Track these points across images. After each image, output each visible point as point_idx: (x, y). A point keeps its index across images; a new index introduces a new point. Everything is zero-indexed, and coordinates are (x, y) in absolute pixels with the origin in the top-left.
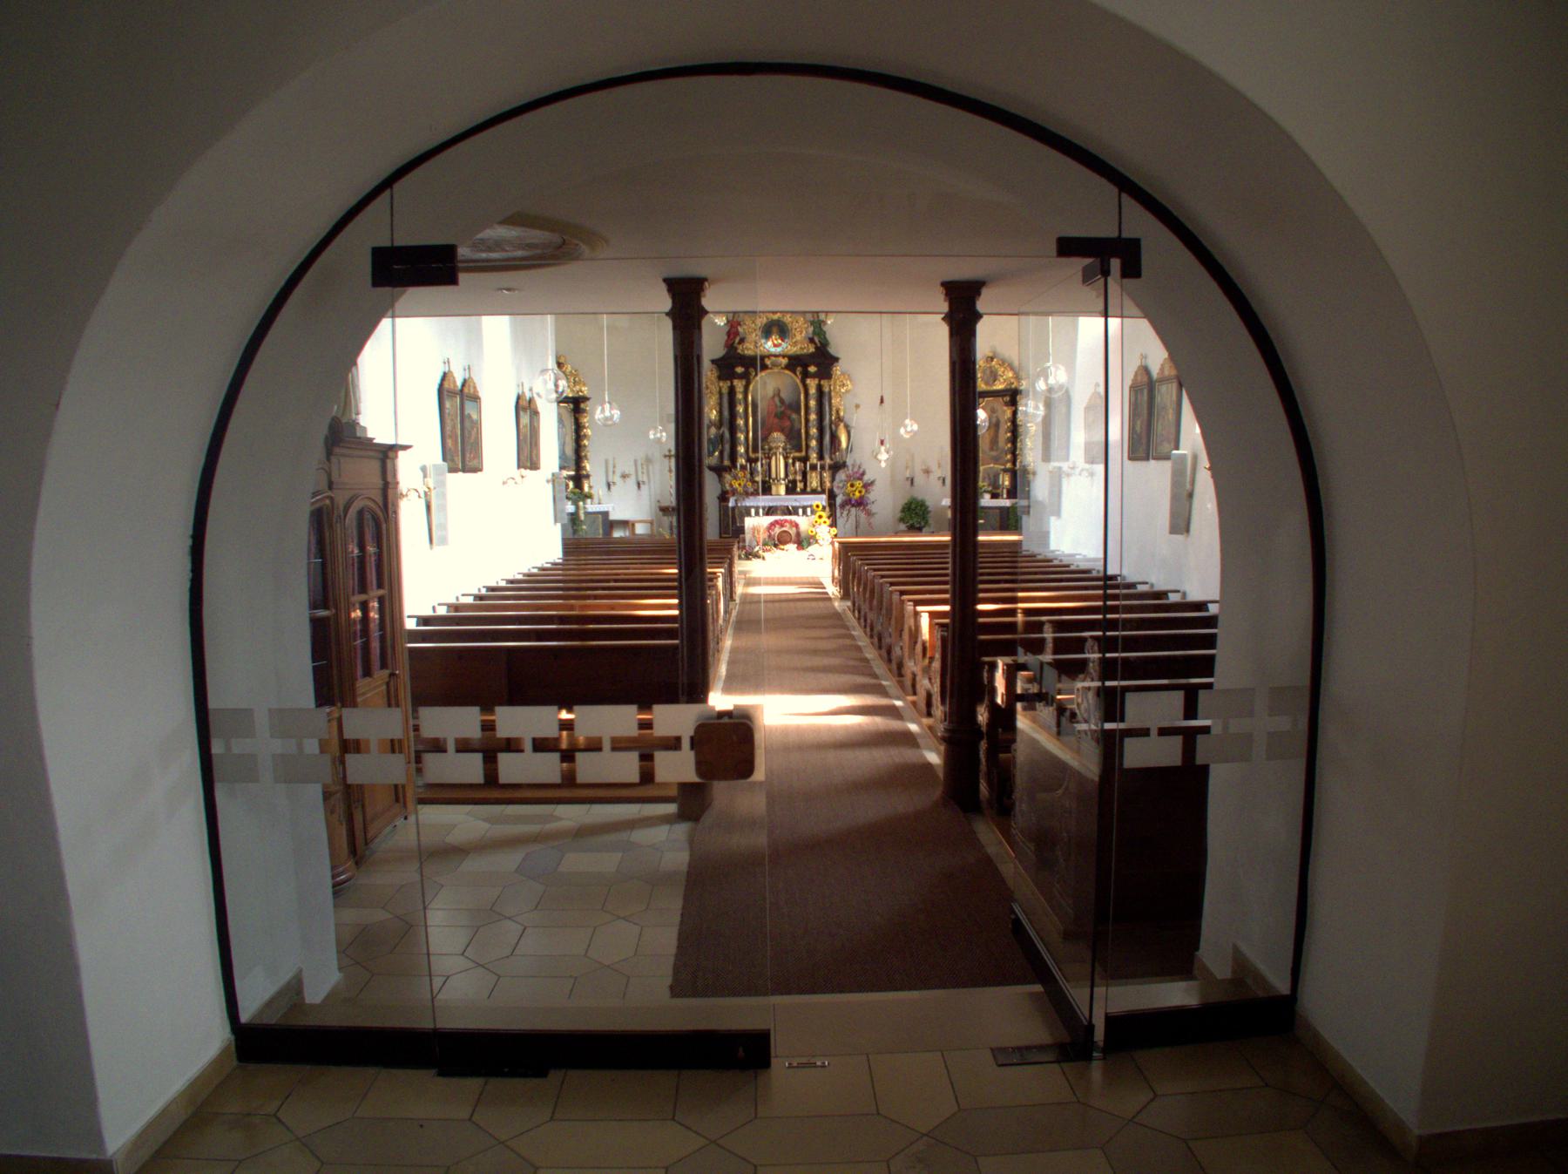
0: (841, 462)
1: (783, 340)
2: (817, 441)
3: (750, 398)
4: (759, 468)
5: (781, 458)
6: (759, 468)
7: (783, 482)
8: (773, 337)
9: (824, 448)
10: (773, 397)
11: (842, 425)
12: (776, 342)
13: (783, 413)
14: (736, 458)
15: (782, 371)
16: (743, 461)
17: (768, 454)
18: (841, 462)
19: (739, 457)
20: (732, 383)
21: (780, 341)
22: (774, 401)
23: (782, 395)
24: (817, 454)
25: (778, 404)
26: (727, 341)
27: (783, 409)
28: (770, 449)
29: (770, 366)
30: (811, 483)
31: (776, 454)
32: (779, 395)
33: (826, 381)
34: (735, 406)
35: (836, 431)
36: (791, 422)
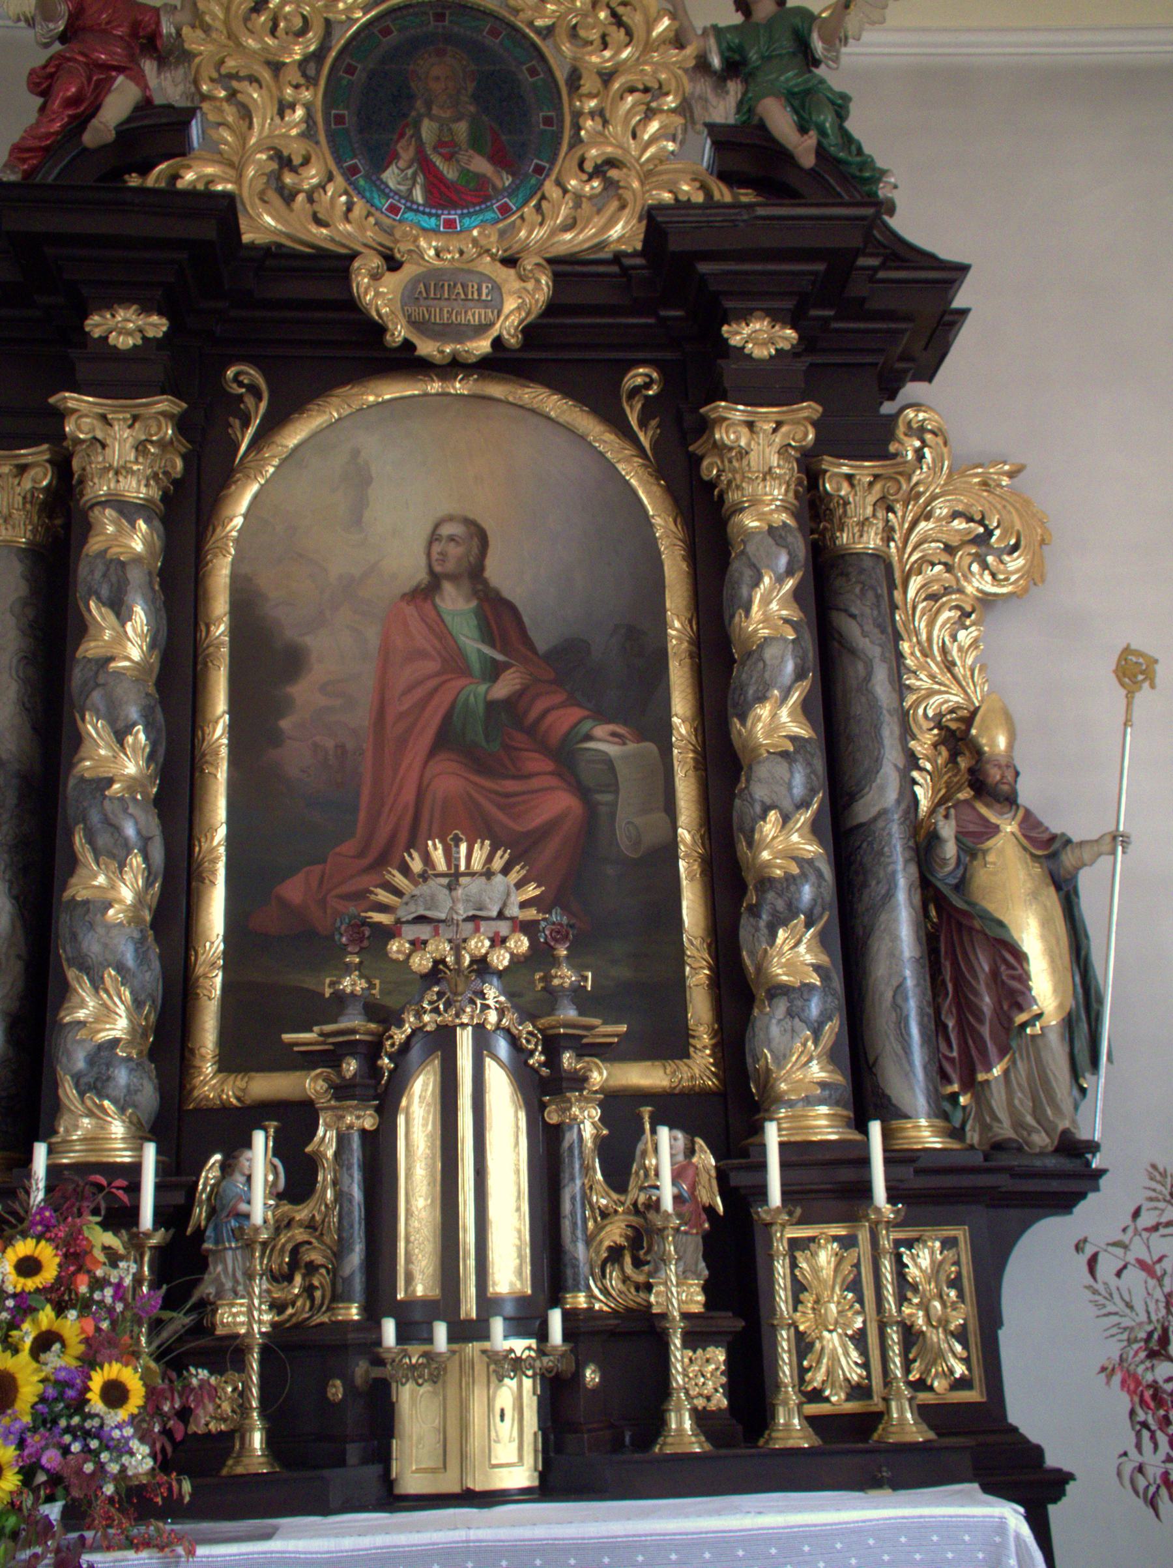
0: (1041, 1140)
1: (500, 159)
2: (823, 940)
3: (221, 572)
4: (259, 1208)
5: (499, 1083)
6: (259, 1208)
7: (521, 1346)
8: (428, 130)
9: (882, 1021)
10: (429, 590)
11: (1009, 827)
12: (449, 172)
13: (511, 707)
14: (56, 1107)
15: (496, 390)
16: (118, 1128)
17: (371, 1051)
18: (1041, 1140)
19: (68, 1092)
20: (62, 466)
21: (481, 165)
22: (440, 630)
23: (496, 572)
24: (832, 1057)
25: (472, 644)
26: (32, 127)
27: (502, 689)
28: (387, 1017)
29: (399, 332)
30: (804, 1345)
31: (444, 1040)
32: (475, 574)
33: (865, 470)
34: (83, 628)
35: (962, 885)
36: (583, 792)
